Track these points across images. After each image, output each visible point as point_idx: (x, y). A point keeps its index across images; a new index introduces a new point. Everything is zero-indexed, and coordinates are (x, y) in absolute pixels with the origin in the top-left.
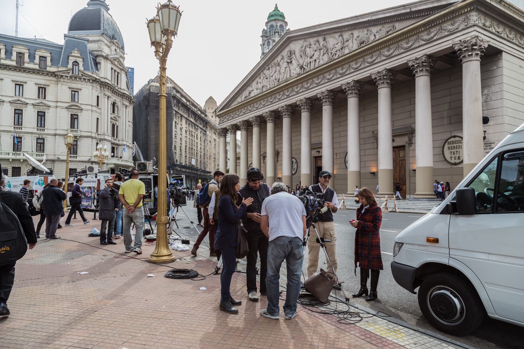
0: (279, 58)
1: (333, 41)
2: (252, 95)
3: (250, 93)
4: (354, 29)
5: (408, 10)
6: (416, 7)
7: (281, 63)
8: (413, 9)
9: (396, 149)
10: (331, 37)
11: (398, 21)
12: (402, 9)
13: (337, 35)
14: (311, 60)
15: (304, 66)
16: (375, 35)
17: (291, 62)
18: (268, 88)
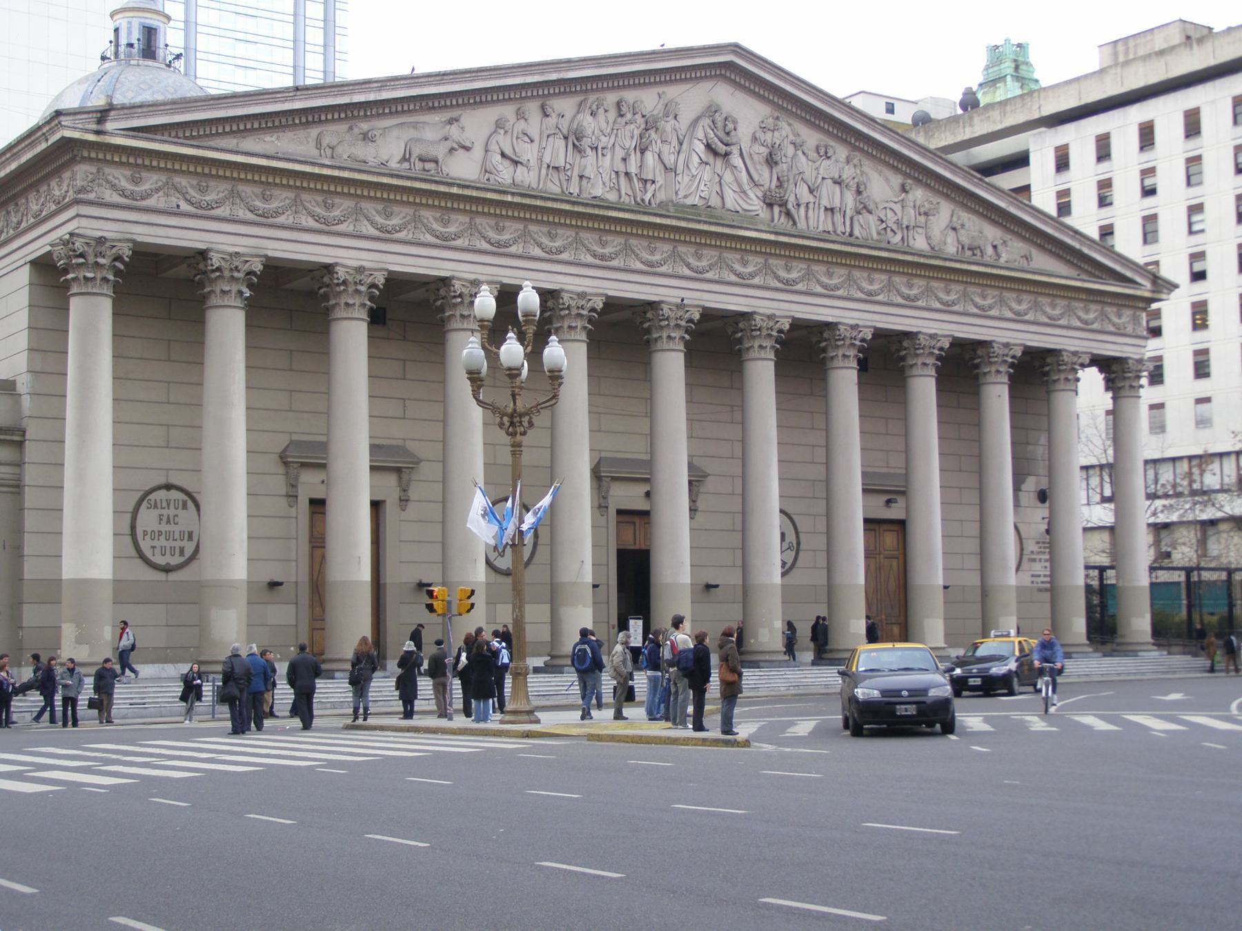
0: (649, 100)
1: (881, 185)
2: (464, 168)
3: (452, 150)
4: (947, 196)
5: (1077, 246)
6: (1090, 248)
7: (668, 125)
8: (1086, 251)
9: (871, 526)
10: (880, 173)
11: (1041, 247)
12: (1069, 236)
13: (896, 180)
14: (812, 199)
15: (790, 206)
16: (995, 247)
17: (727, 154)
18: (598, 192)
